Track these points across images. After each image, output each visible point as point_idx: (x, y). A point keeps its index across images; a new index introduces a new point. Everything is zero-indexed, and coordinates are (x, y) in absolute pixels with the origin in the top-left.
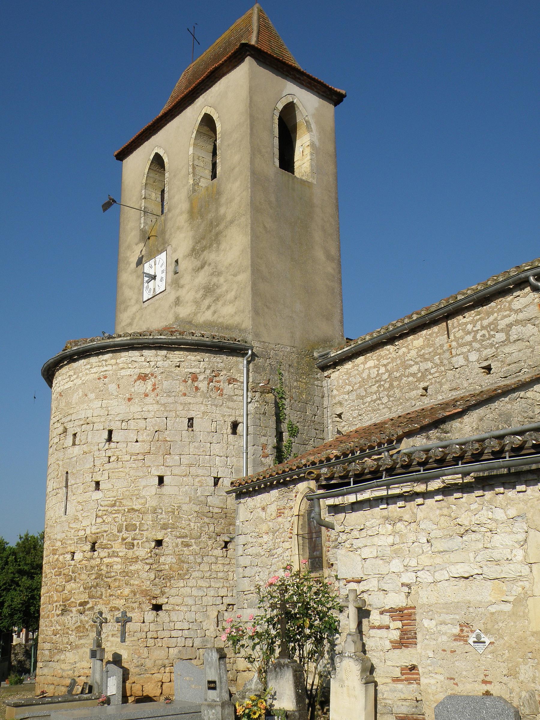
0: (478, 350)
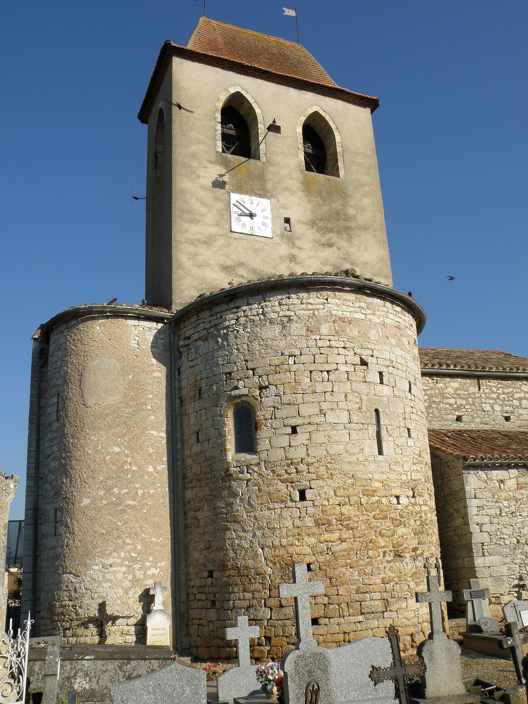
0: (501, 405)
